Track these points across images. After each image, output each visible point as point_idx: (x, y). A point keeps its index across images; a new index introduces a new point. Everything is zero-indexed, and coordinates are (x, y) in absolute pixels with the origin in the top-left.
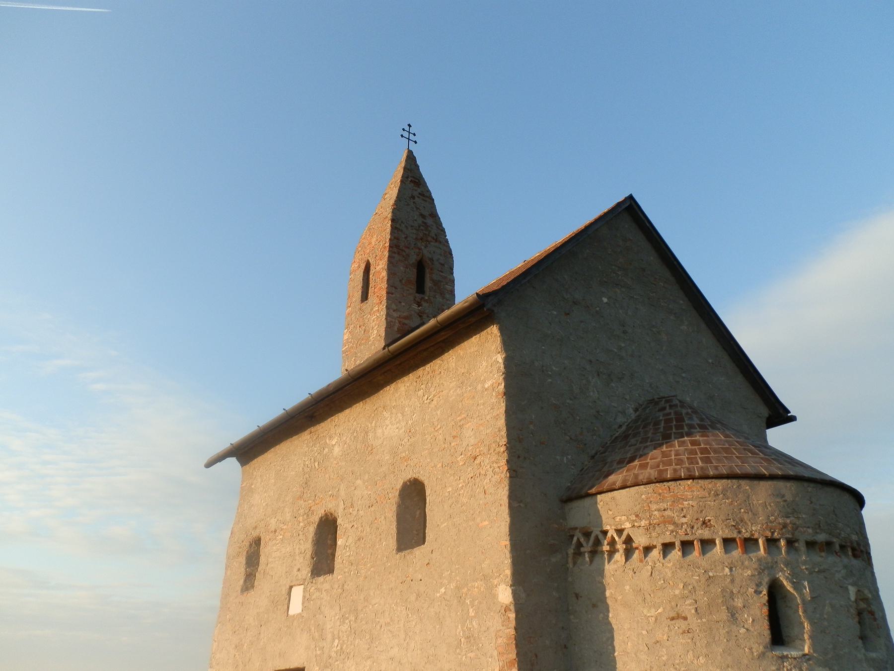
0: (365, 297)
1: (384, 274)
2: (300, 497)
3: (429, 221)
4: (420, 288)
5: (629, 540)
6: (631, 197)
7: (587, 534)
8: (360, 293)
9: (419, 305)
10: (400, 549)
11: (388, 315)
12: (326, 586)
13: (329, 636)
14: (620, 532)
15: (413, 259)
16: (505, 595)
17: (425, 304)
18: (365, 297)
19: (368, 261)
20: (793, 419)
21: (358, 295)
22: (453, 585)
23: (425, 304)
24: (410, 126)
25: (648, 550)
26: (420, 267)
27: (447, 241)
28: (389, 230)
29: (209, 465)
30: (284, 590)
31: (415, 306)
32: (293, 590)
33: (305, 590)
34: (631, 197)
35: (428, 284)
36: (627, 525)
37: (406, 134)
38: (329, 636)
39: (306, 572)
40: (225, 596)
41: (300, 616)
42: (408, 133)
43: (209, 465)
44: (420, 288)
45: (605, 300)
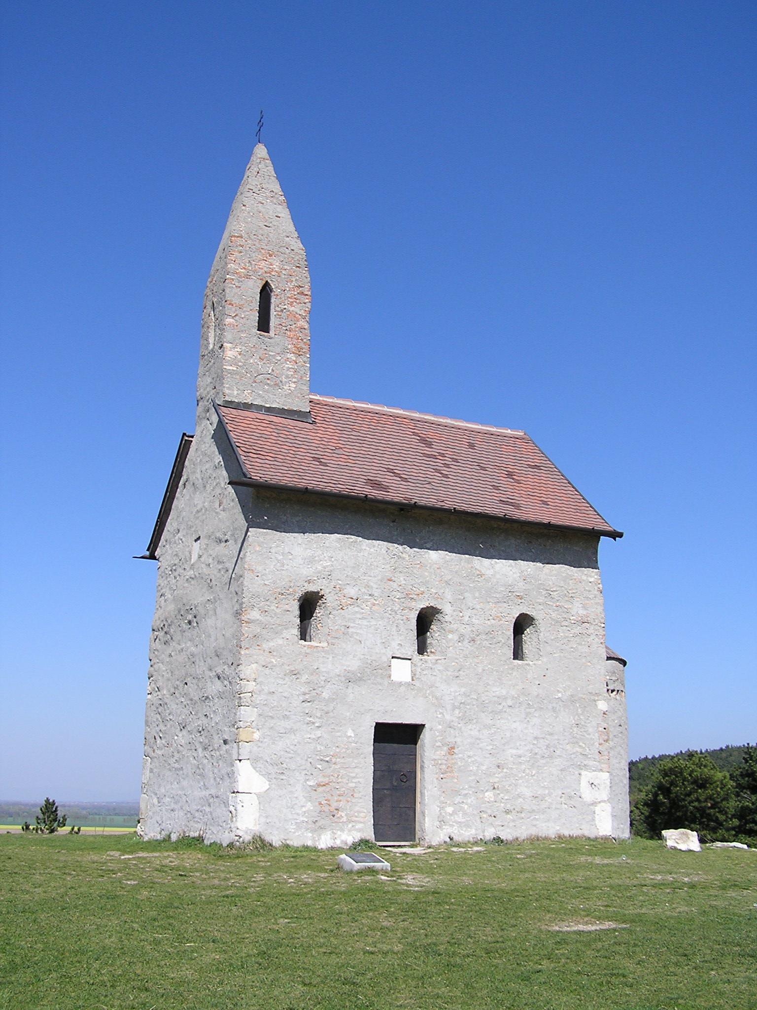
0: (264, 325)
18: (264, 325)
19: (267, 281)
38: (449, 707)
41: (408, 684)
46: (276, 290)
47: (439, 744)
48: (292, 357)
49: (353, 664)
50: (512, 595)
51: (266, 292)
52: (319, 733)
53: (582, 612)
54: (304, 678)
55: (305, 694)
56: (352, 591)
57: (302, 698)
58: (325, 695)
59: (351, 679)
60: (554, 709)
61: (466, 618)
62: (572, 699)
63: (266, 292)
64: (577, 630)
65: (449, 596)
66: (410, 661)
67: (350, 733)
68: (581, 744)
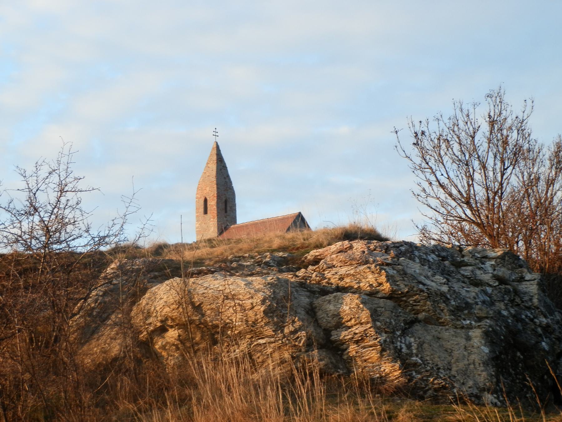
0: (206, 212)
1: (215, 207)
3: (227, 180)
4: (226, 212)
6: (300, 213)
9: (226, 217)
11: (218, 224)
15: (224, 199)
17: (228, 217)
18: (206, 212)
21: (202, 210)
23: (228, 217)
26: (226, 202)
27: (233, 187)
28: (215, 188)
31: (225, 219)
34: (300, 213)
35: (228, 208)
37: (214, 133)
44: (226, 212)
46: (208, 199)
48: (212, 220)
51: (206, 201)
63: (206, 201)
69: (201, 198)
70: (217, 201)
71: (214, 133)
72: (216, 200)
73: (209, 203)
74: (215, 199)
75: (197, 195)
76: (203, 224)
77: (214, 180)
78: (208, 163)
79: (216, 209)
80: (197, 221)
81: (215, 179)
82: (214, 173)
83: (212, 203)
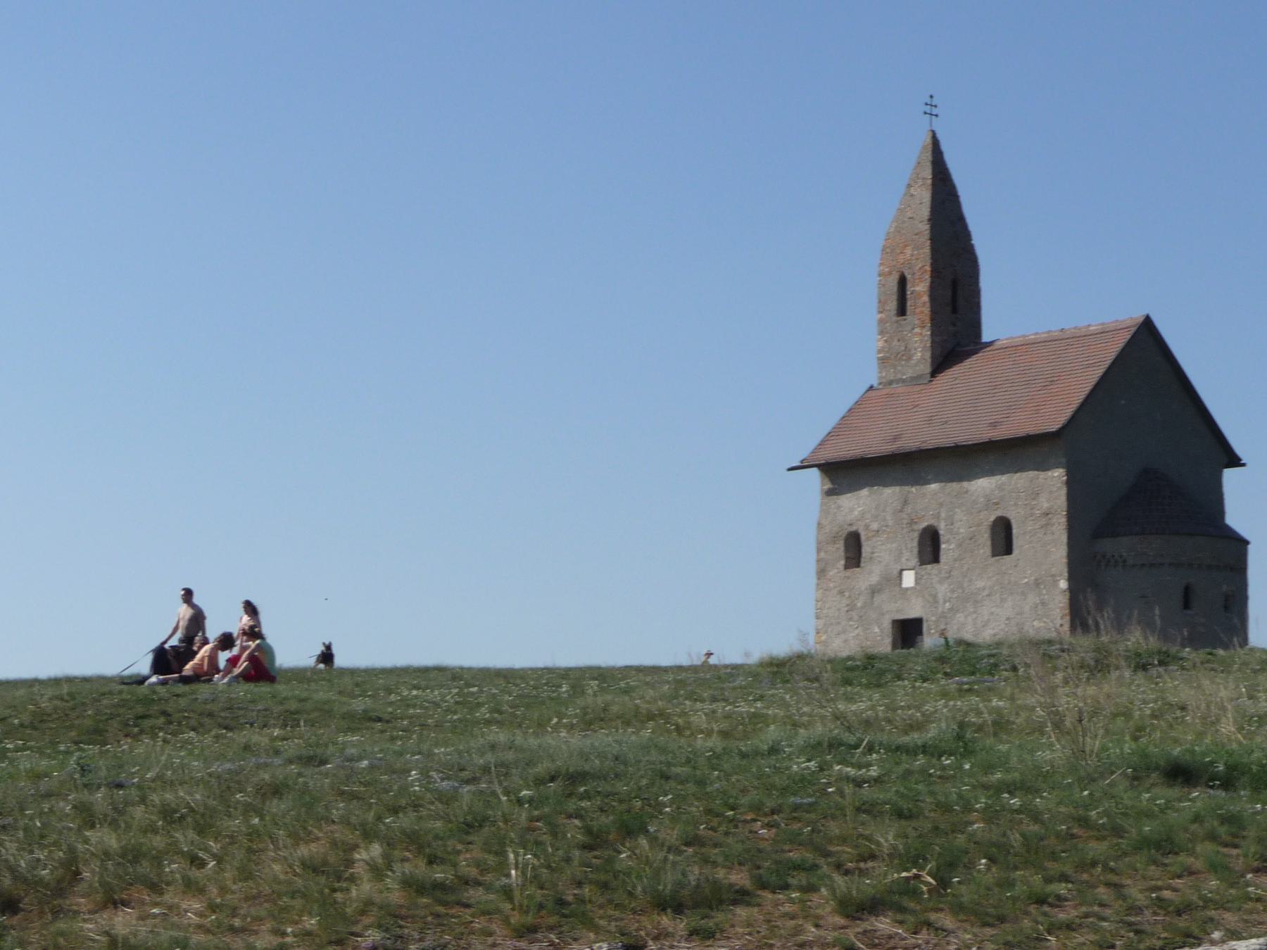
1: (926, 298)
2: (901, 511)
4: (955, 310)
5: (1125, 561)
7: (1104, 557)
8: (895, 303)
9: (954, 325)
10: (994, 555)
12: (935, 572)
13: (941, 601)
14: (1121, 556)
16: (1063, 584)
18: (902, 310)
20: (1244, 465)
21: (893, 305)
22: (1033, 578)
24: (931, 97)
25: (1134, 566)
26: (955, 285)
28: (927, 250)
29: (790, 469)
30: (895, 572)
32: (905, 573)
33: (916, 573)
36: (1124, 554)
37: (928, 109)
38: (941, 601)
39: (914, 561)
40: (821, 573)
41: (912, 588)
42: (931, 110)
43: (790, 469)
45: (1123, 402)
46: (909, 277)
47: (933, 631)
48: (917, 330)
49: (874, 579)
50: (990, 503)
51: (903, 282)
52: (856, 632)
53: (1046, 505)
54: (847, 594)
55: (848, 605)
56: (875, 526)
57: (846, 609)
58: (859, 605)
59: (874, 591)
60: (1023, 593)
61: (955, 530)
62: (1037, 583)
63: (903, 282)
64: (1043, 521)
65: (943, 515)
66: (912, 573)
67: (877, 630)
68: (1045, 620)
69: (890, 273)
70: (932, 283)
71: (928, 109)
72: (929, 280)
73: (910, 289)
74: (927, 276)
75: (882, 268)
76: (895, 343)
77: (925, 228)
78: (909, 186)
79: (928, 305)
80: (881, 333)
81: (928, 227)
82: (925, 212)
83: (920, 288)
